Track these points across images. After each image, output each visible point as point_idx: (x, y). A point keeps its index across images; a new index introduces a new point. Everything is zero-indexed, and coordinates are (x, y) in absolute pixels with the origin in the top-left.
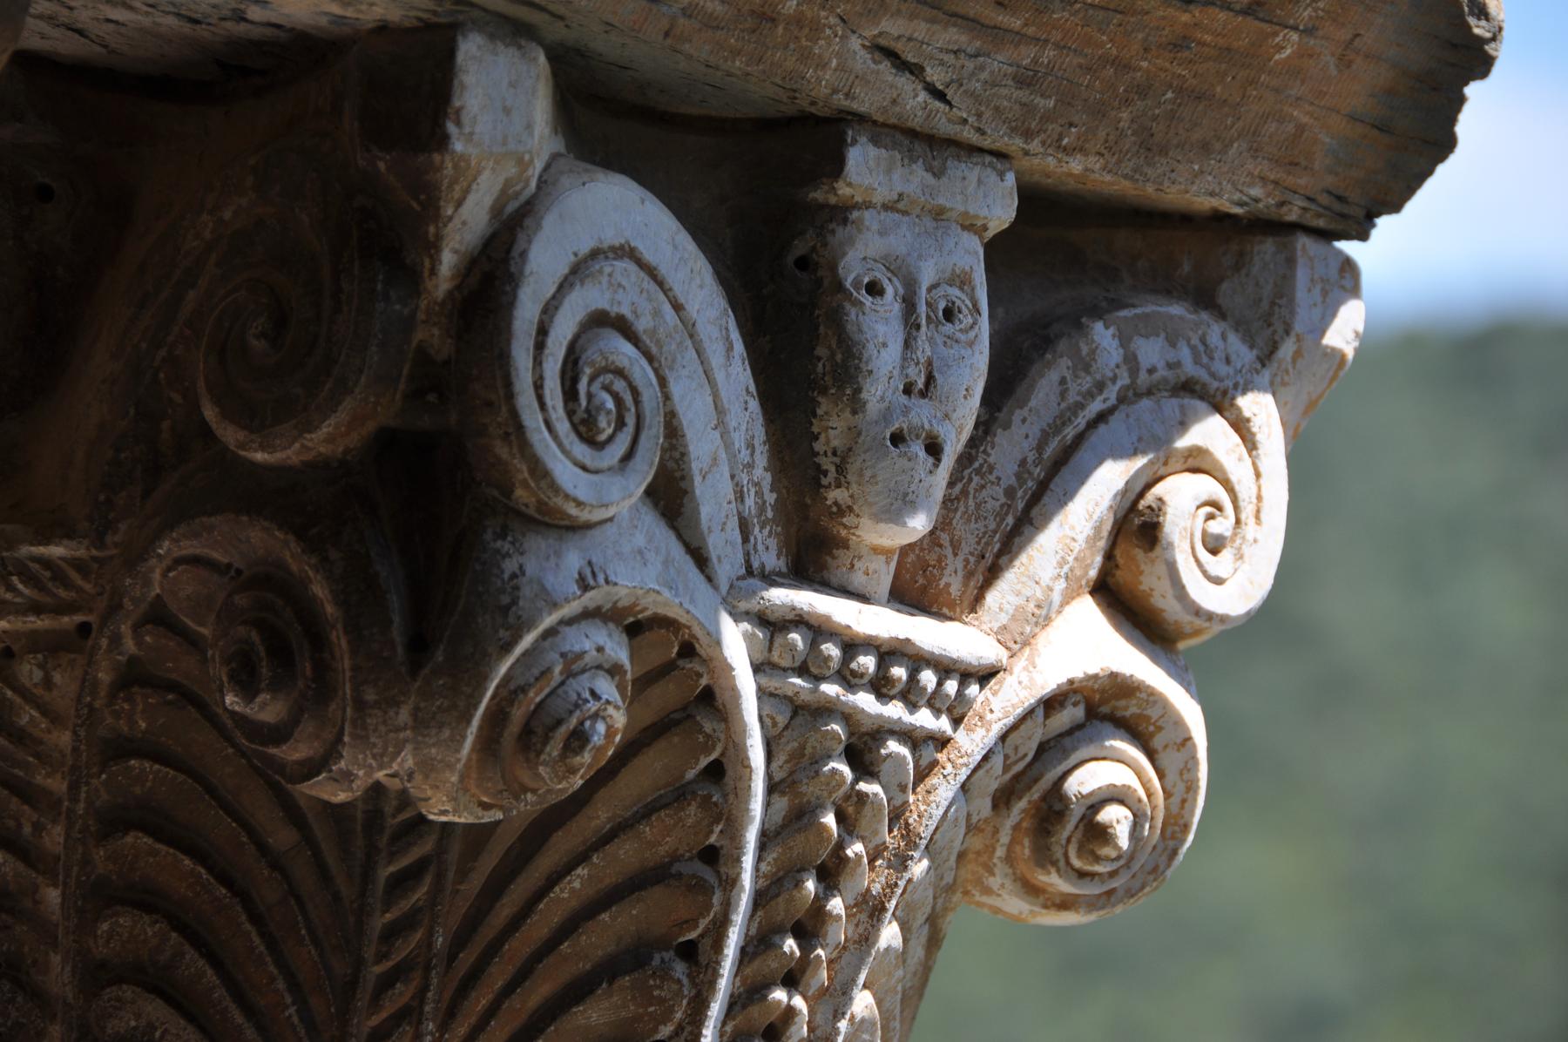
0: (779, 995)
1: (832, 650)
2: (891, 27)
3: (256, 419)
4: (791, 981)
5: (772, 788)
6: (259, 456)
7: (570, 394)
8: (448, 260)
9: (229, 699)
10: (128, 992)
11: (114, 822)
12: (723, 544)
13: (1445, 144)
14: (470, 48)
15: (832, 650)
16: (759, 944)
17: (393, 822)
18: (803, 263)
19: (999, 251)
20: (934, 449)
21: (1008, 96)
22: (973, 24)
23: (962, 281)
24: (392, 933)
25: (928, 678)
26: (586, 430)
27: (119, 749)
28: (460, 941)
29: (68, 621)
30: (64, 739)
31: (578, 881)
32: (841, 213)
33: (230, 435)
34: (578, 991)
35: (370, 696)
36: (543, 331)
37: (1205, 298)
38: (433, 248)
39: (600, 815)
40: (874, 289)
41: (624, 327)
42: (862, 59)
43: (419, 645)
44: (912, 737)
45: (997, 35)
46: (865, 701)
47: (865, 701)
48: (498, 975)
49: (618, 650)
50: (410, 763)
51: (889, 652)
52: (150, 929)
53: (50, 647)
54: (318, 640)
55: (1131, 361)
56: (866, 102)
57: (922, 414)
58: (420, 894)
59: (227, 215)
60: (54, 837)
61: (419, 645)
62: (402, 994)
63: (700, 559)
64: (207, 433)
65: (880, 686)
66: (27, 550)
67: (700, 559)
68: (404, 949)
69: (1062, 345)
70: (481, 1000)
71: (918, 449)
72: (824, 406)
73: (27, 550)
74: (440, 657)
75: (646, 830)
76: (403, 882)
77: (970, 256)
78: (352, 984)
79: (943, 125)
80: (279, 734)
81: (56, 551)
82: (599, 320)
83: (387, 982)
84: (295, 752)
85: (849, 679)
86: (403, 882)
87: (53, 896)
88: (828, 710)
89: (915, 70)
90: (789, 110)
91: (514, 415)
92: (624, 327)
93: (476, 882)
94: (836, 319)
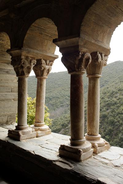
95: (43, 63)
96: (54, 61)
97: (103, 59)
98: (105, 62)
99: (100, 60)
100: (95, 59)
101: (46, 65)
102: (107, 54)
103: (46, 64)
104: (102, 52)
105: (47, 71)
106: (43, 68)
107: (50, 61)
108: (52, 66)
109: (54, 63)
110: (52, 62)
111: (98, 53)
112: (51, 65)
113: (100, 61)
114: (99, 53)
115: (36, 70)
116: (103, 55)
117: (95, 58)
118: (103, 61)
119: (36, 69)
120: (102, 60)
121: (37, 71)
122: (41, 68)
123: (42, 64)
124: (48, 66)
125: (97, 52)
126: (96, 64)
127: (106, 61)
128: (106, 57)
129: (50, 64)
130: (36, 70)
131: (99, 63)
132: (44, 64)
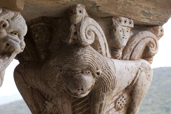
95: (90, 41)
96: (165, 27)
101: (114, 56)
103: (114, 49)
105: (123, 101)
106: (89, 81)
107: (139, 27)
108: (155, 58)
109: (161, 42)
110: (147, 33)
112: (147, 55)
115: (44, 98)
119: (42, 87)
121: (49, 106)
122: (77, 83)
123: (78, 44)
124: (131, 64)
129: (141, 48)
130: (44, 98)
132: (96, 45)
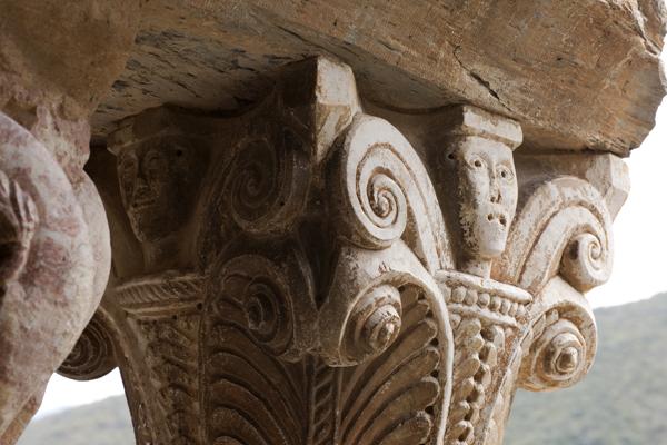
0: (464, 423)
1: (474, 294)
2: (478, 68)
3: (249, 215)
4: (467, 418)
5: (456, 348)
6: (254, 231)
7: (371, 198)
8: (320, 149)
9: (250, 325)
10: (225, 439)
11: (218, 377)
12: (431, 257)
13: (650, 124)
14: (323, 65)
15: (474, 294)
16: (455, 404)
17: (316, 370)
18: (451, 156)
19: (516, 153)
20: (503, 222)
21: (518, 95)
22: (506, 69)
23: (507, 164)
24: (320, 410)
25: (508, 304)
26: (378, 212)
27: (217, 350)
28: (345, 414)
29: (193, 305)
30: (196, 347)
31: (386, 387)
32: (463, 136)
33: (243, 224)
34: (391, 428)
35: (302, 318)
36: (358, 173)
37: (582, 176)
38: (313, 143)
39: (393, 362)
40: (477, 164)
41: (388, 173)
42: (468, 79)
43: (320, 299)
44: (504, 326)
45: (513, 74)
46: (486, 312)
47: (486, 312)
48: (361, 425)
49: (396, 297)
50: (320, 344)
51: (494, 294)
52: (232, 414)
53: (189, 314)
54: (281, 299)
55: (562, 195)
56: (470, 95)
57: (498, 208)
58: (329, 396)
59: (239, 145)
60: (195, 385)
61: (320, 299)
62: (325, 432)
63: (424, 263)
64: (238, 228)
65: (492, 307)
66: (177, 279)
67: (424, 263)
68: (325, 417)
69: (539, 190)
70: (355, 433)
71: (497, 221)
72: (464, 206)
73: (177, 279)
74: (328, 301)
75: (412, 367)
76: (321, 393)
77: (508, 154)
78: (307, 430)
79: (497, 107)
80: (270, 338)
81: (188, 278)
82: (380, 171)
83: (319, 429)
84: (275, 345)
85: (481, 304)
86: (321, 393)
87: (196, 405)
88: (472, 316)
89: (486, 84)
90: (443, 103)
91: (350, 205)
92: (388, 173)
93: (350, 389)
94: (465, 176)
97: (498, 241)
98: (557, 293)
99: (400, 261)
100: (280, 250)
102: (589, 135)
104: (462, 82)
111: (335, 87)
113: (411, 292)
114: (375, 100)
116: (472, 149)
117: (278, 221)
118: (481, 278)
120: (464, 251)
125: (298, 83)
126: (315, 370)
127: (569, 266)
128: (560, 189)
131: (362, 333)
